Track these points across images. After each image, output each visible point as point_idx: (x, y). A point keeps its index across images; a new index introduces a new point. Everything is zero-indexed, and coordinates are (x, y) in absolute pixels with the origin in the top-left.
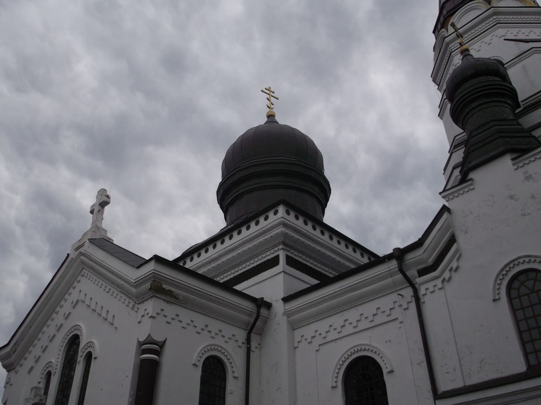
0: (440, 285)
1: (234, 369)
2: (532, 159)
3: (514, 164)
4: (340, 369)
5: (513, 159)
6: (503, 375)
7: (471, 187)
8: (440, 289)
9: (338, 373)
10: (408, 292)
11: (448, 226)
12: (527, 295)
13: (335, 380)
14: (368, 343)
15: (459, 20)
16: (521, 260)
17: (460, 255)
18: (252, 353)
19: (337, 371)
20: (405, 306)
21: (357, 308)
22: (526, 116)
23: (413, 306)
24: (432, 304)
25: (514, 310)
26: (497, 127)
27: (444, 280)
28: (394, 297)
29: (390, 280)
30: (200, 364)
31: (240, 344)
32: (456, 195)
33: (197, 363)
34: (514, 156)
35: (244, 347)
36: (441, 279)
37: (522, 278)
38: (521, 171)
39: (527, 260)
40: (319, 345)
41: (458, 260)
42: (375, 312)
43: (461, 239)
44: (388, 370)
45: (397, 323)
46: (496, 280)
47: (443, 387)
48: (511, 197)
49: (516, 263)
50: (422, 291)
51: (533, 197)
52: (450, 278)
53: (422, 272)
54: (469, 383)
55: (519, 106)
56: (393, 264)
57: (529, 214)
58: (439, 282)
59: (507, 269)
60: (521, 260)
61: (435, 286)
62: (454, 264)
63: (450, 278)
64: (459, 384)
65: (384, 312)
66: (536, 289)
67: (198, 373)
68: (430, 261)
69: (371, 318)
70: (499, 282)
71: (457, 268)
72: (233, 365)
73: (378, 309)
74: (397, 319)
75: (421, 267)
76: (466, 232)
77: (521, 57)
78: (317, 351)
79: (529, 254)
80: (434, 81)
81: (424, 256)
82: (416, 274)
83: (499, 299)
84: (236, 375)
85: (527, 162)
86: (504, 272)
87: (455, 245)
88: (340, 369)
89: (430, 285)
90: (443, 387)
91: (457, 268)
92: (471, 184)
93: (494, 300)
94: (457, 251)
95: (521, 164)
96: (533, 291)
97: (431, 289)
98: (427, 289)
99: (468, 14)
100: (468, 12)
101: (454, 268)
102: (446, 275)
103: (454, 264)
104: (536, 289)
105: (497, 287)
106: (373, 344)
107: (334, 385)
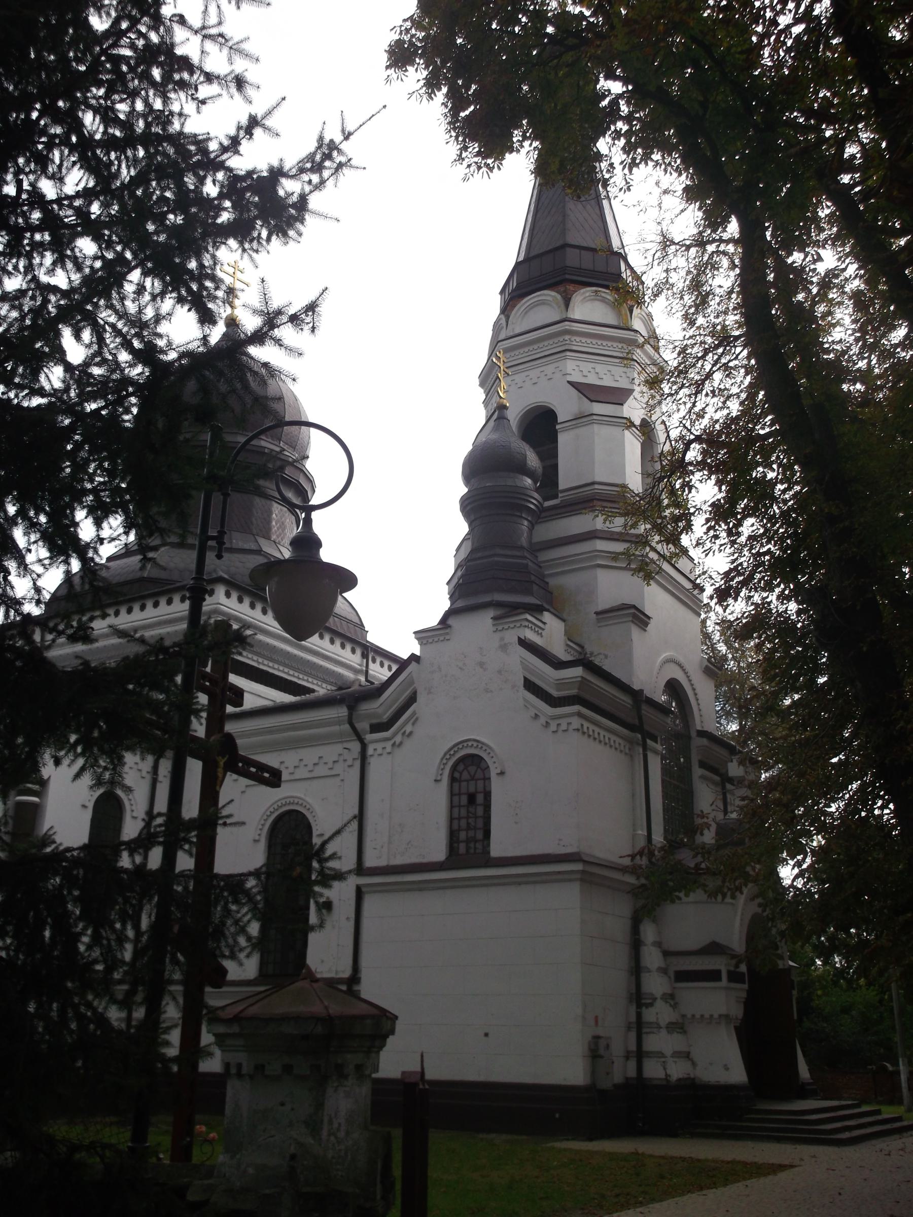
0: (389, 749)
1: (134, 808)
2: (512, 626)
3: (494, 625)
4: (265, 820)
5: (494, 618)
6: (425, 860)
7: (447, 637)
8: (389, 753)
9: (263, 825)
10: (356, 747)
11: (410, 682)
12: (467, 781)
13: (259, 832)
14: (302, 796)
15: (526, 313)
16: (470, 744)
17: (417, 719)
18: (158, 785)
19: (263, 822)
20: (349, 762)
21: (298, 750)
22: (554, 522)
23: (358, 764)
24: (376, 766)
25: (452, 794)
26: (496, 559)
27: (394, 745)
28: (338, 748)
29: (337, 728)
30: (91, 805)
31: (144, 774)
32: (430, 640)
33: (87, 804)
34: (499, 612)
35: (149, 777)
36: (392, 742)
37: (461, 767)
38: (499, 635)
39: (475, 744)
40: (247, 786)
41: (413, 724)
42: (316, 761)
43: (421, 698)
44: (318, 833)
45: (338, 779)
46: (442, 759)
47: (370, 861)
48: (481, 665)
49: (465, 744)
50: (370, 751)
51: (500, 672)
52: (401, 744)
53: (376, 728)
54: (398, 861)
55: (556, 497)
56: (343, 711)
57: (491, 691)
58: (388, 745)
59: (456, 749)
60: (470, 744)
61: (384, 748)
62: (408, 728)
63: (401, 744)
64: (382, 863)
65: (326, 763)
66: (477, 777)
67: (88, 815)
68: (385, 718)
69: (310, 767)
70: (445, 761)
71: (411, 733)
72: (132, 802)
73: (320, 758)
74: (339, 775)
75: (374, 721)
76: (429, 693)
77: (581, 420)
78: (243, 792)
79: (478, 738)
80: (482, 384)
81: (380, 711)
82: (368, 728)
83: (440, 780)
84: (135, 814)
85: (506, 627)
86: (452, 752)
87: (415, 705)
88: (265, 820)
89: (379, 746)
90: (370, 861)
91: (411, 733)
92: (447, 634)
93: (436, 781)
94: (414, 713)
95: (500, 628)
96: (473, 778)
97: (379, 751)
98: (375, 750)
99: (536, 309)
100: (537, 305)
101: (407, 733)
102: (398, 739)
103: (408, 728)
104: (477, 777)
105: (442, 767)
106: (308, 799)
107: (257, 838)
